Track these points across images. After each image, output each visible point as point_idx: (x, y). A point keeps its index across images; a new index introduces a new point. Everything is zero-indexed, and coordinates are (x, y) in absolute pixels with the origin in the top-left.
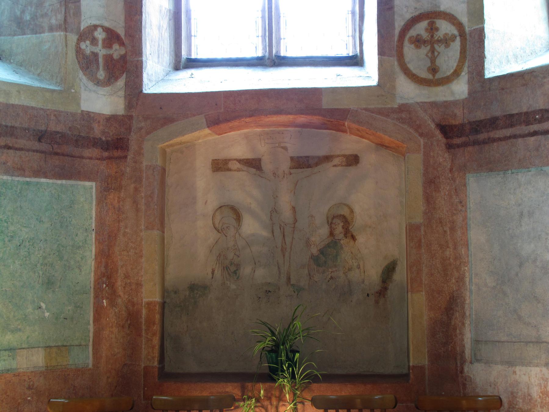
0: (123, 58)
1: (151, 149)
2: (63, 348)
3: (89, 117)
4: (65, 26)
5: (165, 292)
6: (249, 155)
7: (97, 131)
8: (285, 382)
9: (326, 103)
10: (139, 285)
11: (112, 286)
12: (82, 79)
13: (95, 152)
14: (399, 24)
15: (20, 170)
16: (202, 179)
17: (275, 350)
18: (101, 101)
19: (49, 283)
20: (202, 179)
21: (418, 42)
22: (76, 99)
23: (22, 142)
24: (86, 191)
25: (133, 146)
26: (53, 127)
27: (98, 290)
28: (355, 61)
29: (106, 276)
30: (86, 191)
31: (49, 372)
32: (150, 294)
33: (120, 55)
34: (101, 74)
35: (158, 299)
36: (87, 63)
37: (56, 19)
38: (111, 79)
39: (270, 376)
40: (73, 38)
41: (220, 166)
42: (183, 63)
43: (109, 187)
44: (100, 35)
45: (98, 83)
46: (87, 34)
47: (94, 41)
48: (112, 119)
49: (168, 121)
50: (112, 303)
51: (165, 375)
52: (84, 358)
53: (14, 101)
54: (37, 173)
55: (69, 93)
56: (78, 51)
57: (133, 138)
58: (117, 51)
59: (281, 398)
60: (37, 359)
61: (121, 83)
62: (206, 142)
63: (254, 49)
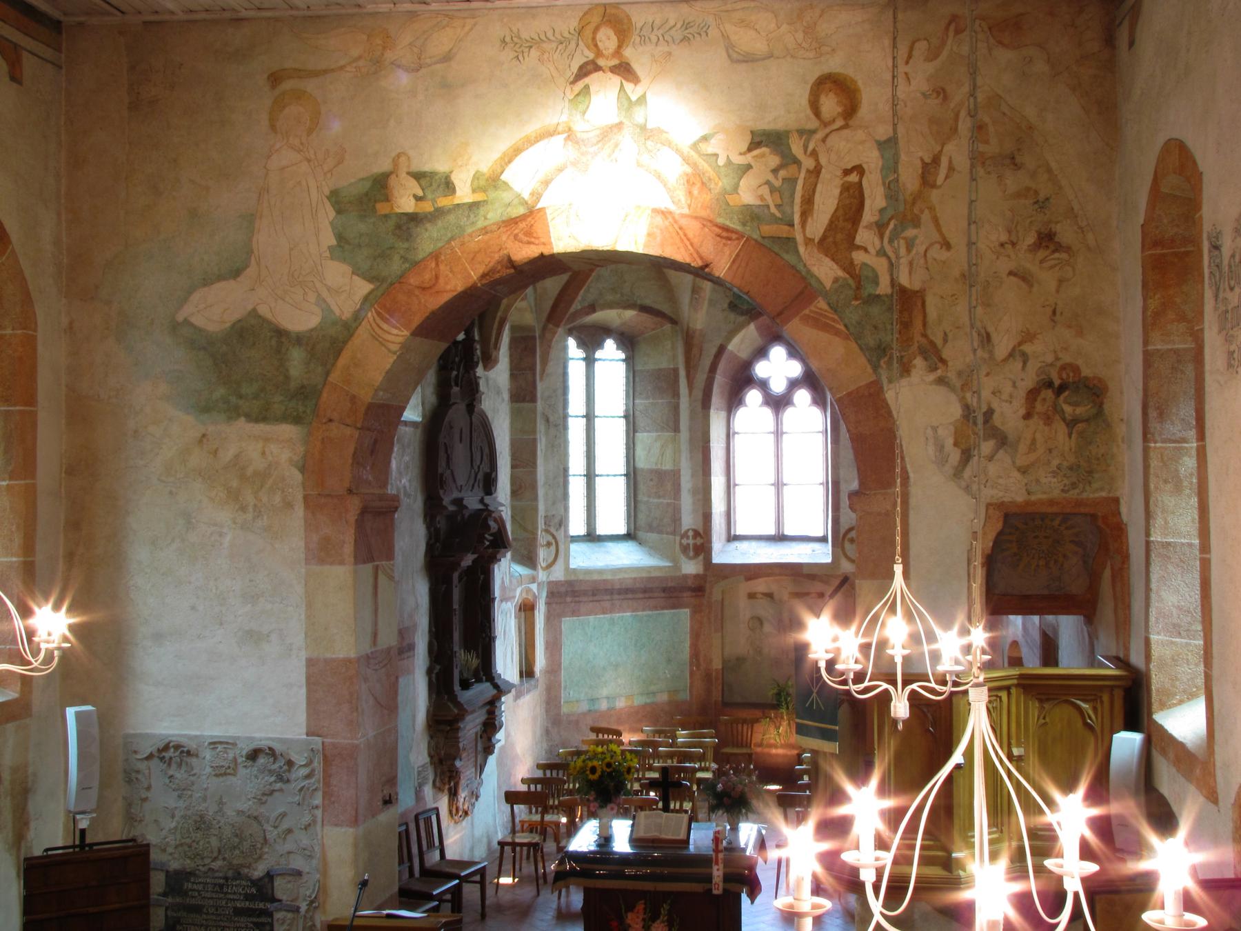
0: (702, 544)
1: (716, 593)
2: (676, 691)
3: (686, 577)
4: (674, 533)
5: (724, 662)
6: (766, 591)
7: (690, 583)
8: (784, 711)
9: (805, 571)
10: (711, 660)
11: (698, 660)
12: (683, 559)
13: (689, 594)
14: (842, 531)
15: (656, 608)
16: (743, 603)
17: (779, 694)
18: (691, 568)
19: (669, 661)
20: (743, 603)
21: (852, 541)
22: (679, 569)
23: (656, 595)
24: (685, 613)
25: (708, 591)
26: (670, 584)
27: (691, 664)
28: (823, 539)
29: (695, 654)
30: (685, 613)
31: (670, 703)
32: (717, 664)
33: (701, 545)
34: (691, 554)
35: (720, 667)
36: (685, 549)
37: (670, 529)
38: (697, 554)
39: (776, 707)
40: (678, 538)
41: (752, 596)
42: (732, 538)
43: (696, 610)
44: (691, 534)
45: (690, 558)
46: (685, 535)
47: (688, 538)
48: (696, 576)
49: (725, 577)
50: (698, 666)
51: (726, 704)
52: (685, 696)
53: (654, 574)
54: (663, 608)
55: (677, 567)
56: (681, 544)
57: (708, 585)
58: (699, 541)
59: (782, 718)
60: (664, 697)
61: (701, 557)
62: (744, 587)
63: (771, 531)
